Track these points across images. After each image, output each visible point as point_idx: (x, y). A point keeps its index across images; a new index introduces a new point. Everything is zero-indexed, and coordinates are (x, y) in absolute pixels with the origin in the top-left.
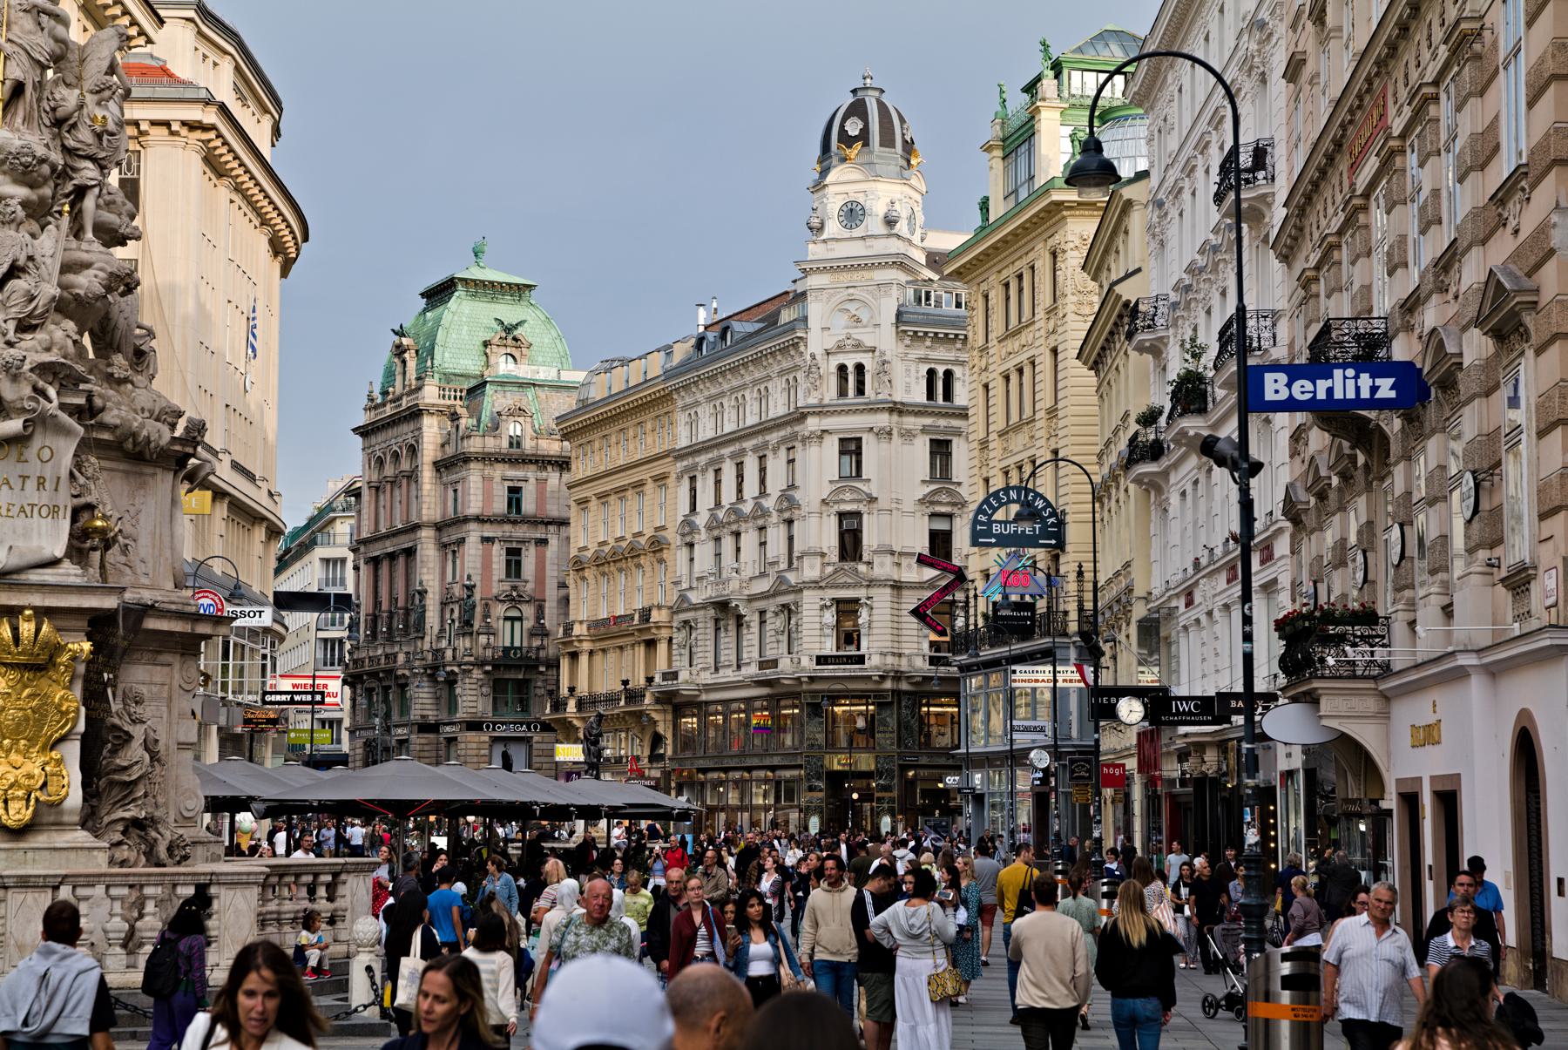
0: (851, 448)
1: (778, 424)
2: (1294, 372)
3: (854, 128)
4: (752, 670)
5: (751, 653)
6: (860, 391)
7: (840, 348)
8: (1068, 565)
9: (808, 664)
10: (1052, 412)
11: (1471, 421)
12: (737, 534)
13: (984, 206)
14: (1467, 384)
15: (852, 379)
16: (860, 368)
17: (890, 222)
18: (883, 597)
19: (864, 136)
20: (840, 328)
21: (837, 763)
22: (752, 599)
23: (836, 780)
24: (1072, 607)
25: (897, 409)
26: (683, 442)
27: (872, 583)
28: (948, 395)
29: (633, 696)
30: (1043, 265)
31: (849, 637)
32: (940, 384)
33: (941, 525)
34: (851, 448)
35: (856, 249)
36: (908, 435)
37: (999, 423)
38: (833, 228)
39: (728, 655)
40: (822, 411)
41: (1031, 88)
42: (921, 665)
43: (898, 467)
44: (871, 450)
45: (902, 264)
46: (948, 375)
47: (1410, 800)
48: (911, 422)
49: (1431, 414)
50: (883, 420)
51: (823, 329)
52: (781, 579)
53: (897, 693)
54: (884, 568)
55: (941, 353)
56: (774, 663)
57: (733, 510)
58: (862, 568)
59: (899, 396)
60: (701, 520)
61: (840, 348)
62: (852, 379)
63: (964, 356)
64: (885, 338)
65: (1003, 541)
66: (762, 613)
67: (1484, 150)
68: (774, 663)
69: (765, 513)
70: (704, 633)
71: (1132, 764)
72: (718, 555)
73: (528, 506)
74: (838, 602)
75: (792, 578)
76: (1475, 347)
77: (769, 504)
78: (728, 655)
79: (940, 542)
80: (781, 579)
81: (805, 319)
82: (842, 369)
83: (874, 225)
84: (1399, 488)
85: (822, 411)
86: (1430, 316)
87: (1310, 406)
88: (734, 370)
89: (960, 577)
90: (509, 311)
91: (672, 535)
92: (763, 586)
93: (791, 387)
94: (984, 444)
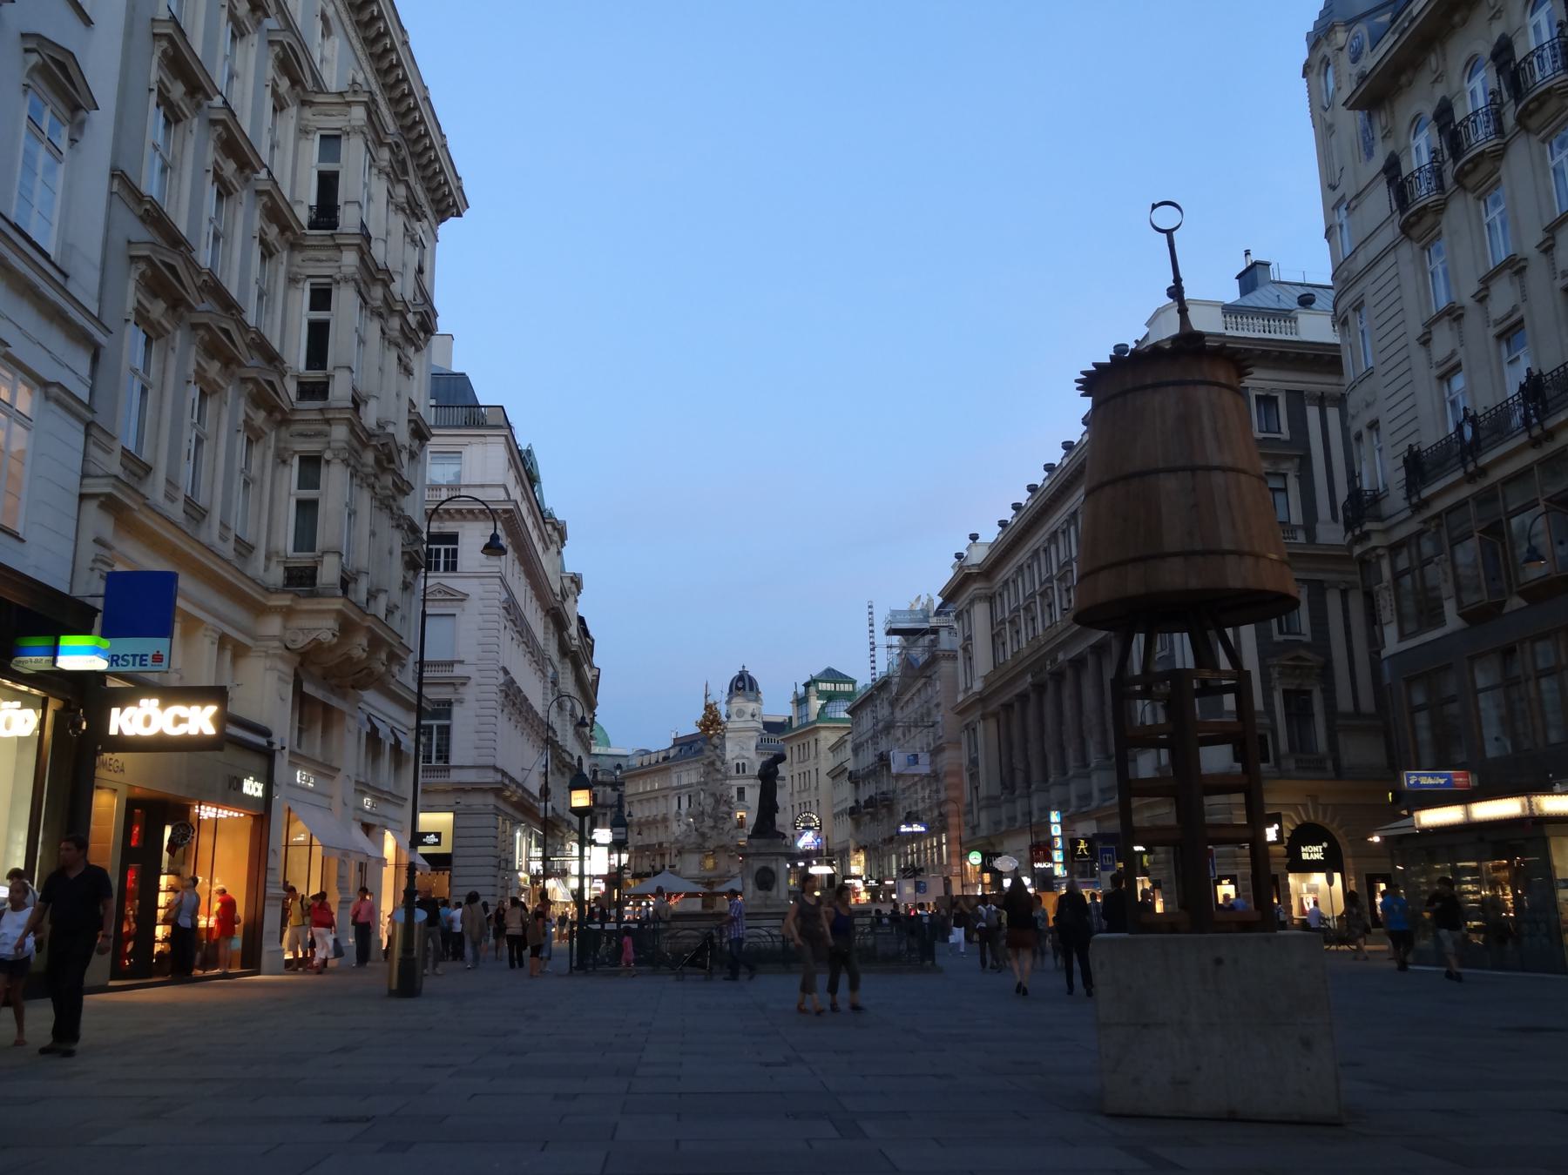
20: (737, 751)
26: (675, 784)
30: (812, 743)
41: (807, 685)
62: (740, 768)
91: (672, 815)
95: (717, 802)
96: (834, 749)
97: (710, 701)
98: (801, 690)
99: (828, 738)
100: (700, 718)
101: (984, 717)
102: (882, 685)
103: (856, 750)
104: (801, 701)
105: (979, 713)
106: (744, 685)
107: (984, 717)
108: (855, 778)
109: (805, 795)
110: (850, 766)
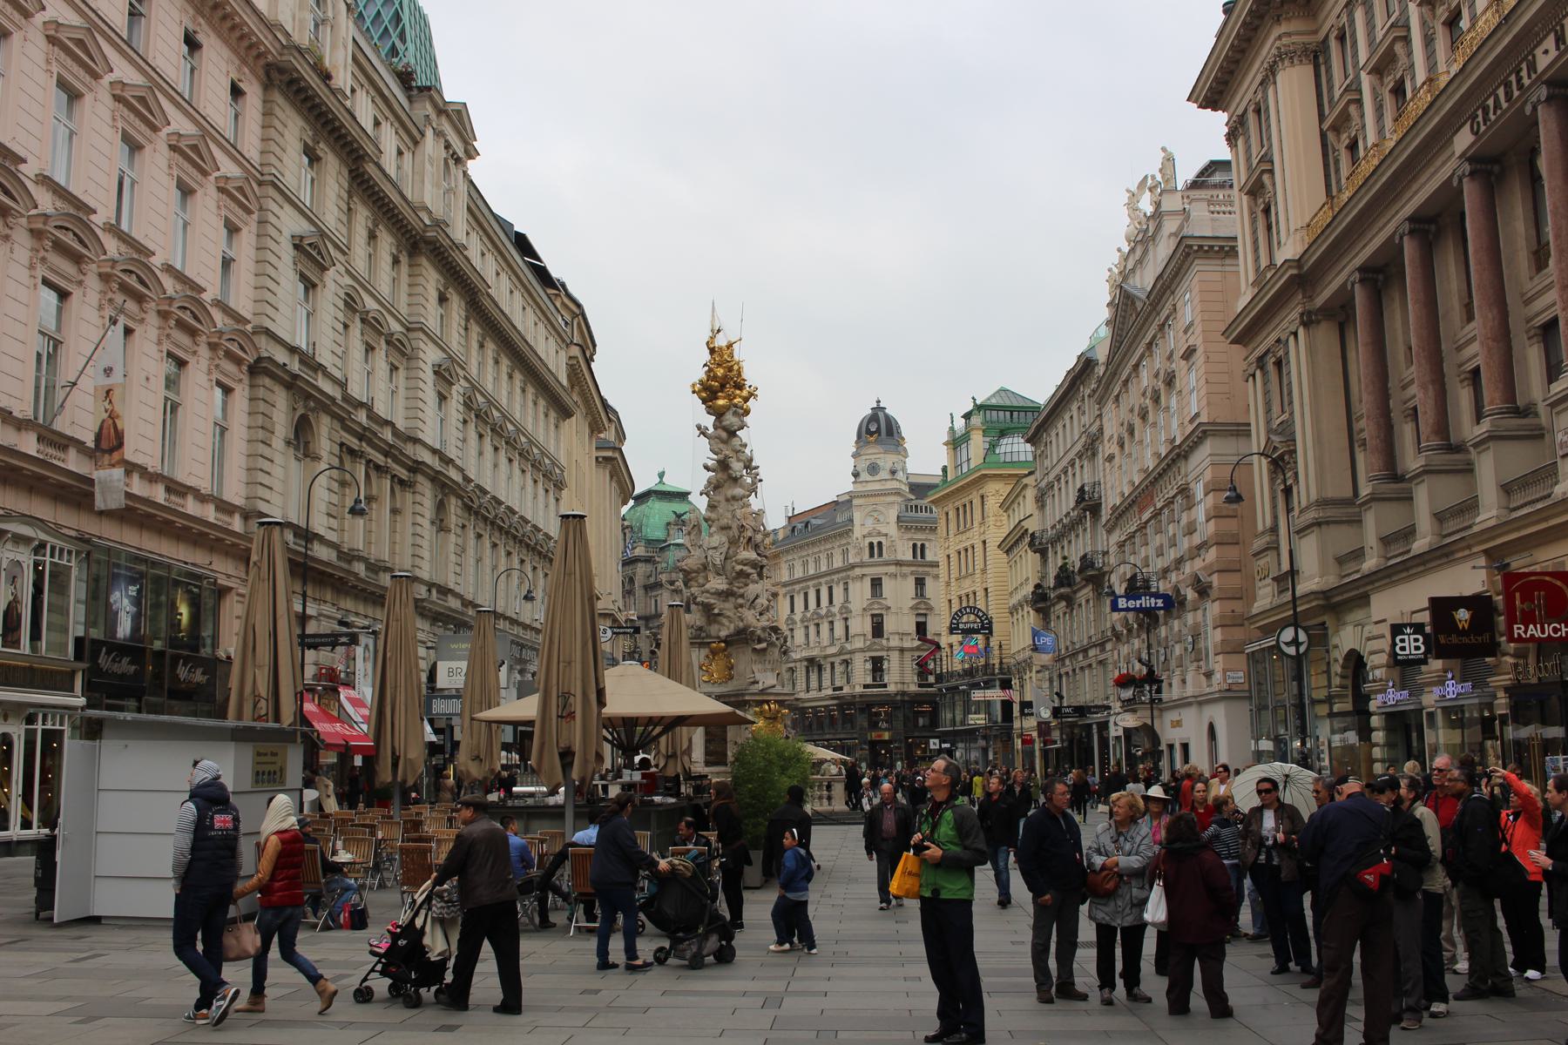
0: (876, 583)
1: (838, 571)
3: (873, 429)
4: (830, 692)
6: (880, 555)
7: (870, 535)
8: (994, 642)
9: (859, 690)
10: (984, 571)
11: (1190, 618)
12: (818, 625)
13: (945, 469)
14: (1189, 606)
15: (875, 549)
16: (880, 544)
17: (893, 472)
18: (895, 656)
19: (878, 431)
20: (870, 523)
21: (874, 735)
22: (826, 657)
23: (873, 745)
24: (996, 662)
25: (899, 563)
26: (785, 578)
27: (889, 649)
28: (923, 556)
30: (977, 502)
32: (919, 550)
33: (921, 619)
34: (876, 583)
35: (877, 486)
37: (954, 574)
39: (814, 684)
40: (862, 565)
41: (967, 416)
43: (899, 592)
44: (886, 583)
45: (898, 493)
46: (923, 546)
47: (1171, 747)
48: (906, 570)
49: (1175, 611)
50: (892, 569)
51: (862, 524)
52: (843, 648)
53: (903, 701)
54: (895, 642)
55: (919, 537)
56: (841, 688)
57: (815, 613)
58: (884, 642)
59: (900, 557)
60: (798, 617)
61: (870, 535)
62: (875, 549)
63: (931, 537)
64: (892, 529)
66: (832, 664)
67: (1191, 530)
68: (841, 688)
69: (834, 615)
70: (800, 675)
71: (1035, 734)
72: (807, 635)
74: (873, 658)
75: (848, 647)
76: (1190, 594)
77: (835, 610)
78: (814, 684)
79: (921, 628)
80: (843, 648)
81: (851, 520)
82: (871, 544)
83: (884, 474)
84: (1163, 634)
85: (862, 565)
86: (1174, 577)
87: (1135, 609)
88: (813, 544)
89: (938, 647)
90: (680, 507)
92: (833, 650)
93: (845, 553)
94: (948, 584)
95: (733, 542)
96: (1007, 505)
97: (721, 341)
98: (960, 424)
99: (996, 492)
100: (701, 374)
101: (1308, 321)
102: (1085, 366)
103: (1040, 501)
104: (956, 442)
105: (1300, 309)
106: (879, 430)
107: (1308, 321)
109: (967, 583)
110: (1033, 526)
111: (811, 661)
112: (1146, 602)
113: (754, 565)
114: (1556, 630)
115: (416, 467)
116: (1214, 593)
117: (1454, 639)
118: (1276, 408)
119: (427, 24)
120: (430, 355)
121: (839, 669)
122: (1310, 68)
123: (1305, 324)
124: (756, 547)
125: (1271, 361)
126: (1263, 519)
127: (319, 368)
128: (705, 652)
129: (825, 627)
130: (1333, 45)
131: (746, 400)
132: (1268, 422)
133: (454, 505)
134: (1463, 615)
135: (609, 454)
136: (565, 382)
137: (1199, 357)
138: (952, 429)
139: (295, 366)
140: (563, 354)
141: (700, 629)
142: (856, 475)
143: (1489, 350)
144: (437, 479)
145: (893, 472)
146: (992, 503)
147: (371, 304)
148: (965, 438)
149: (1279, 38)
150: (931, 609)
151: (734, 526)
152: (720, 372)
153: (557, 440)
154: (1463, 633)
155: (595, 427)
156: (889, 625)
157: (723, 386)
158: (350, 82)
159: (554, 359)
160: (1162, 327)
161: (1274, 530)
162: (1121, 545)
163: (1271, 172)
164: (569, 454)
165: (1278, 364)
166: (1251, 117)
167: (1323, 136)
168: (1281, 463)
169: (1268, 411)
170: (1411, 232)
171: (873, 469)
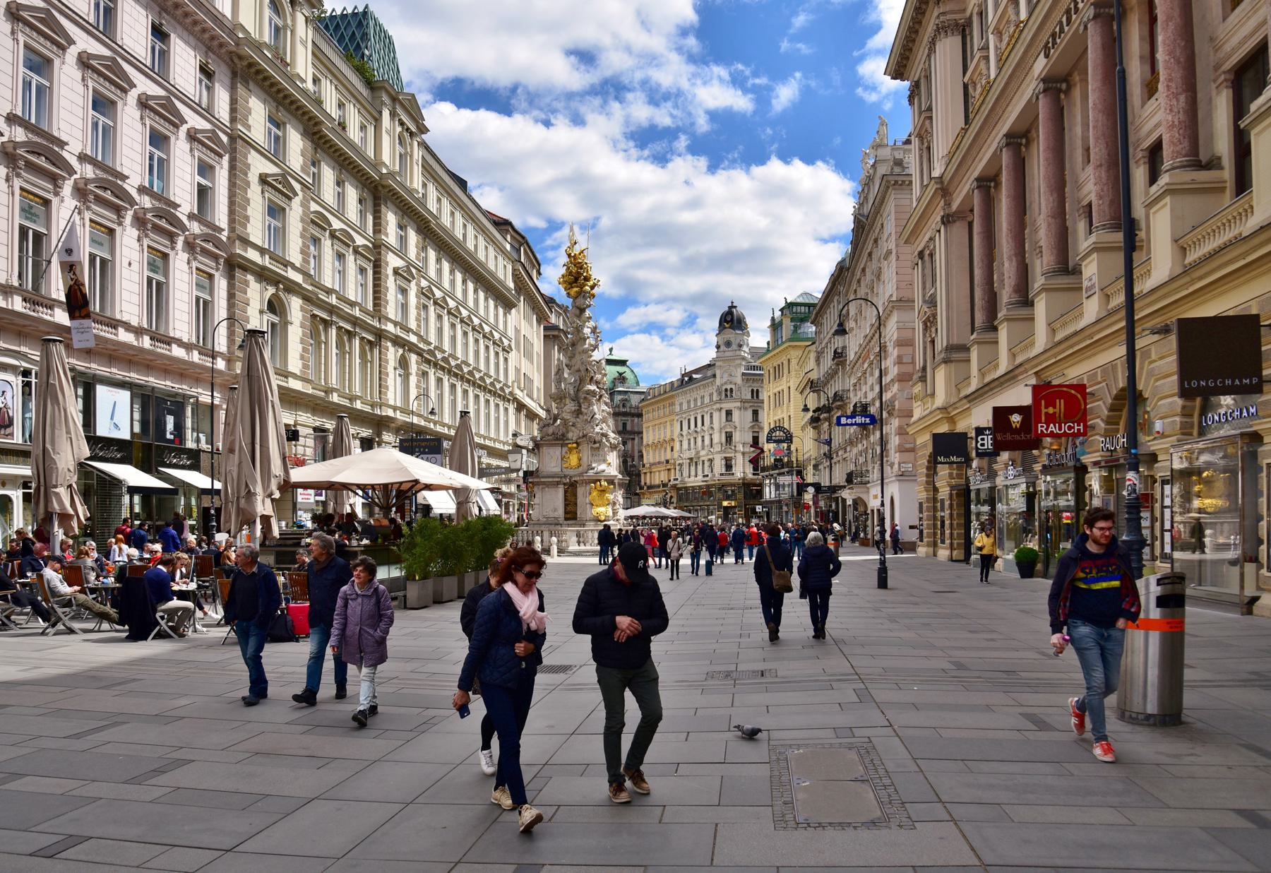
0: (729, 413)
2: (848, 417)
5: (700, 472)
19: (732, 320)
21: (725, 504)
29: (665, 485)
30: (786, 363)
31: (729, 467)
32: (755, 393)
34: (729, 413)
36: (746, 409)
38: (723, 348)
39: (693, 473)
41: (781, 310)
42: (750, 476)
43: (742, 419)
44: (736, 415)
45: (744, 358)
60: (684, 433)
64: (739, 380)
65: (775, 441)
73: (629, 428)
78: (693, 473)
79: (756, 440)
83: (734, 347)
89: (762, 451)
90: (621, 369)
93: (711, 395)
97: (577, 250)
98: (778, 314)
103: (818, 360)
104: (775, 326)
106: (732, 321)
107: (947, 220)
108: (814, 386)
110: (814, 376)
111: (691, 459)
112: (858, 420)
113: (593, 393)
114: (1070, 428)
115: (380, 335)
116: (896, 413)
117: (1009, 437)
118: (928, 285)
119: (391, 42)
120: (393, 261)
121: (707, 464)
122: (957, 40)
123: (943, 223)
124: (597, 383)
125: (927, 252)
126: (919, 363)
127: (287, 264)
128: (565, 449)
129: (699, 440)
130: (975, 20)
131: (592, 288)
132: (924, 296)
133: (413, 358)
134: (1016, 419)
135: (556, 333)
136: (512, 285)
137: (893, 257)
138: (773, 319)
139: (267, 262)
140: (510, 267)
141: (563, 435)
142: (718, 347)
143: (1049, 224)
144: (398, 342)
145: (740, 346)
146: (794, 362)
147: (337, 224)
148: (781, 324)
149: (938, 17)
150: (762, 428)
151: (583, 369)
152: (574, 270)
153: (505, 323)
154: (1017, 431)
155: (542, 318)
156: (737, 437)
157: (576, 280)
158: (311, 70)
159: (503, 271)
160: (876, 241)
161: (924, 369)
162: (855, 385)
163: (931, 118)
164: (517, 331)
165: (931, 255)
166: (923, 82)
167: (966, 87)
168: (929, 323)
169: (924, 288)
170: (1007, 145)
171: (728, 344)
